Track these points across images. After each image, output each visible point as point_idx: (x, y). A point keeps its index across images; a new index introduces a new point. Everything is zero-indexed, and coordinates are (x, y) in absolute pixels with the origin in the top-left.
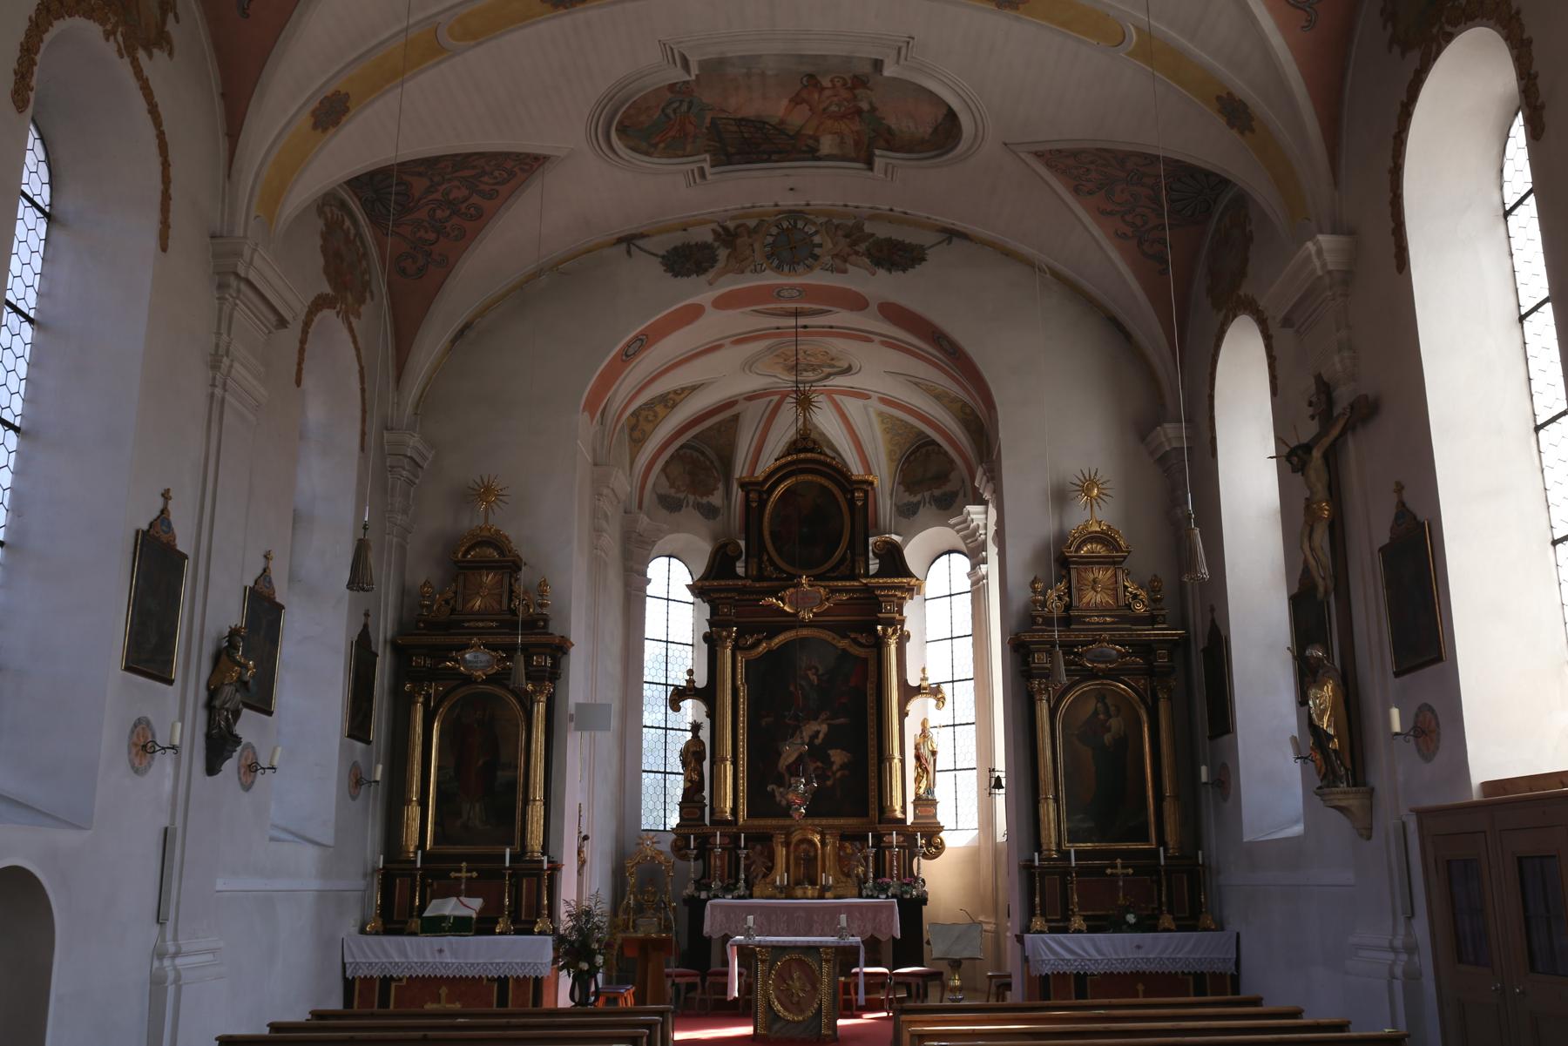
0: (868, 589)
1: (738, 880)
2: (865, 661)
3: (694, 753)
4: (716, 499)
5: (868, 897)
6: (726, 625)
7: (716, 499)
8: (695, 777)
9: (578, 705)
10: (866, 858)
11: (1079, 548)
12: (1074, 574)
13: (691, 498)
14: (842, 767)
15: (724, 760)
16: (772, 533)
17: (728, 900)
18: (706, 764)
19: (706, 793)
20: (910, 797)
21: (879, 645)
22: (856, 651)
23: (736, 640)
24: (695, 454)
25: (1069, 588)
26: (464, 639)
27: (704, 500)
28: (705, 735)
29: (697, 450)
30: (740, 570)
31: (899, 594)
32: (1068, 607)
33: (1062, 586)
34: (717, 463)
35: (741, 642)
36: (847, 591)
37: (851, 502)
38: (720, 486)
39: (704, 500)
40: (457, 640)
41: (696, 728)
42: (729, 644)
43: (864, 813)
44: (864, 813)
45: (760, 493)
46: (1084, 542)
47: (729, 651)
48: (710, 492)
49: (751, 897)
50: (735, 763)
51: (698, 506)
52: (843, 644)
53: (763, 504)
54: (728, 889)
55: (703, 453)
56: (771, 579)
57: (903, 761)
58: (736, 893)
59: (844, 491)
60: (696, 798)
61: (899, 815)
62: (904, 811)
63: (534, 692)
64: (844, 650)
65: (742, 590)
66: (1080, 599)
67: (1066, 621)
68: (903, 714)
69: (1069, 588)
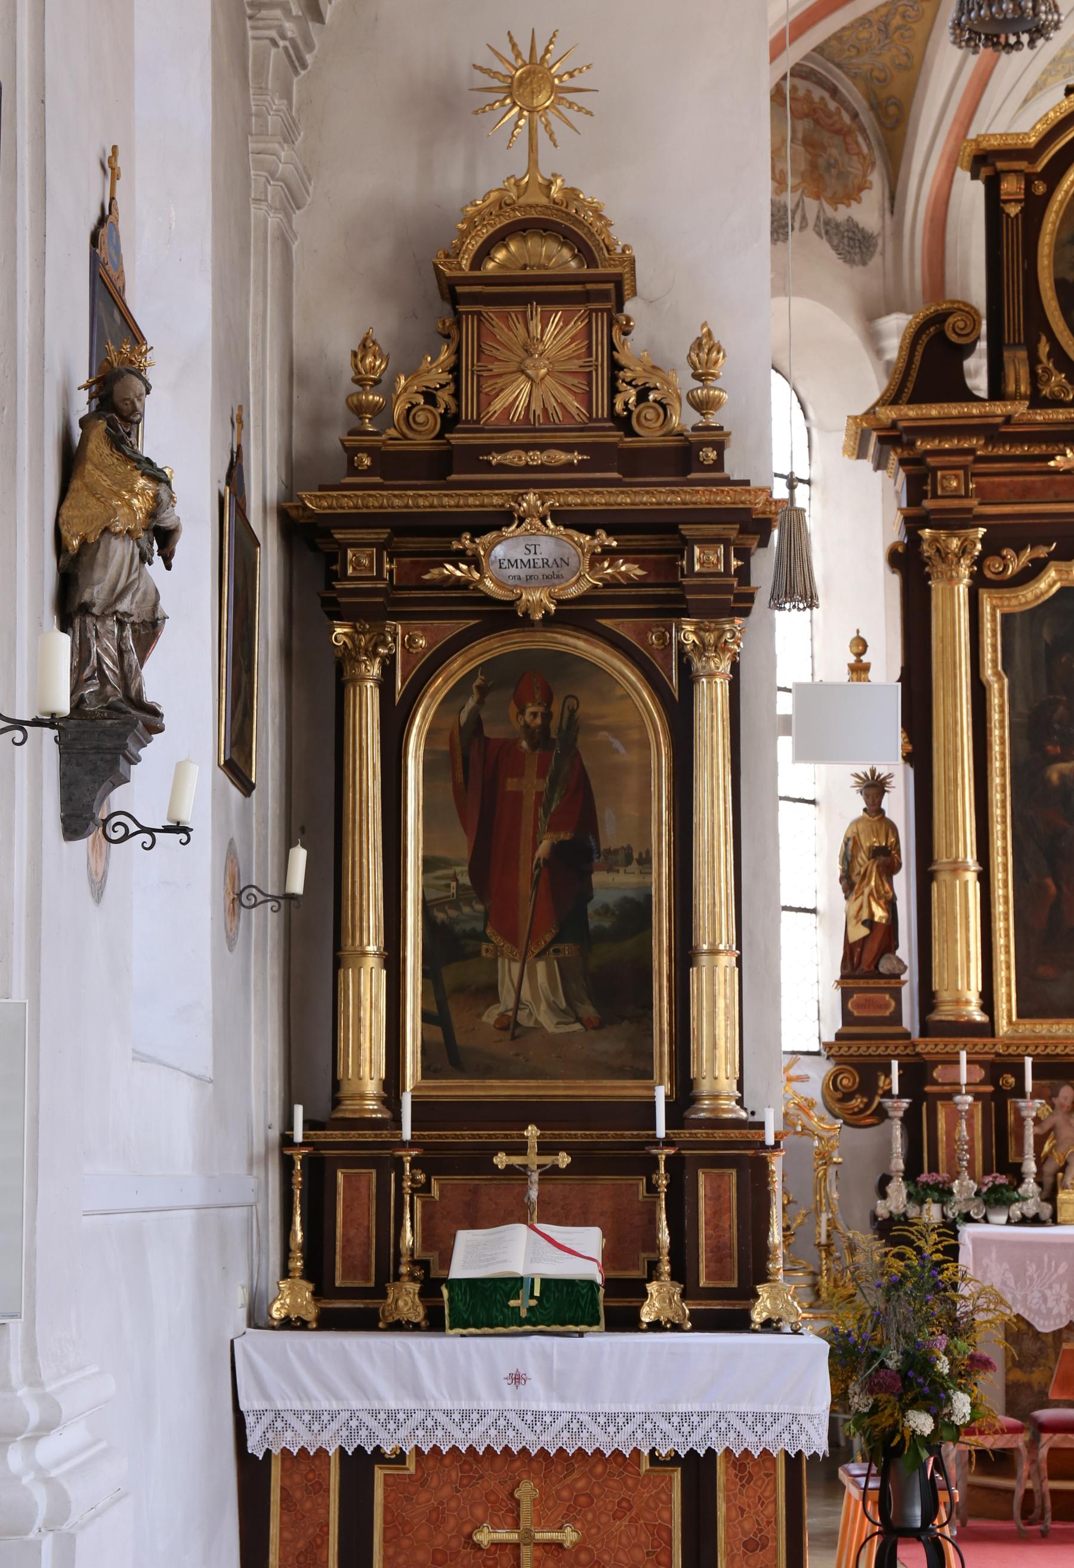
1: (1019, 1178)
3: (876, 853)
4: (867, 212)
6: (955, 521)
7: (867, 212)
8: (879, 914)
9: (800, 691)
13: (812, 206)
15: (957, 868)
16: (1060, 285)
17: (997, 1228)
18: (903, 884)
19: (906, 949)
23: (979, 562)
24: (818, 93)
26: (496, 500)
27: (841, 214)
28: (898, 806)
29: (821, 82)
30: (979, 382)
34: (866, 118)
35: (994, 566)
38: (876, 178)
39: (841, 214)
40: (473, 501)
41: (874, 788)
42: (964, 570)
45: (1029, 179)
47: (962, 590)
48: (851, 194)
49: (1054, 1220)
50: (985, 878)
51: (829, 230)
53: (1035, 208)
54: (996, 1198)
55: (834, 92)
56: (1056, 403)
58: (1016, 1210)
60: (885, 966)
63: (701, 649)
65: (991, 432)
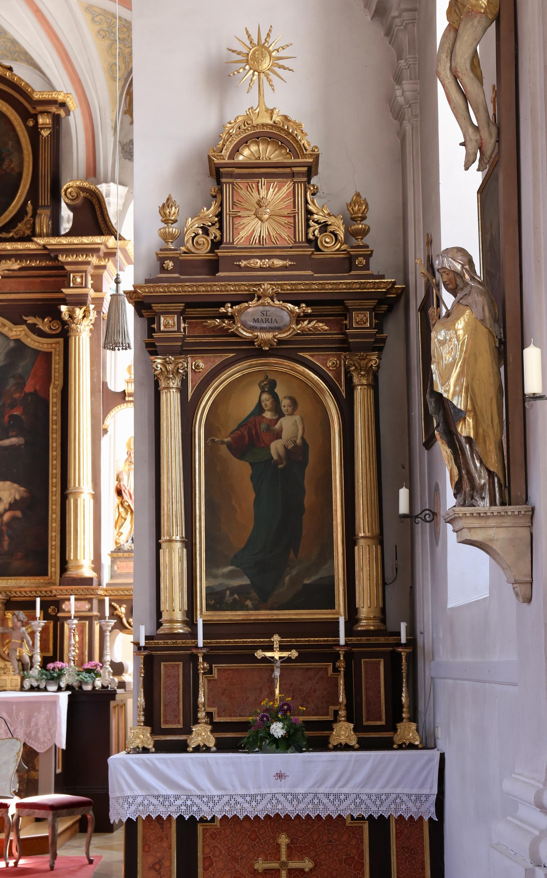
0: (49, 254)
2: (48, 356)
5: (32, 689)
10: (32, 634)
11: (236, 150)
12: (227, 189)
14: (13, 506)
20: (107, 547)
21: (65, 333)
22: (33, 342)
25: (220, 215)
31: (94, 260)
32: (216, 245)
33: (210, 212)
36: (18, 256)
37: (34, 132)
43: (43, 571)
44: (43, 571)
46: (245, 142)
52: (18, 332)
57: (97, 498)
59: (25, 115)
61: (87, 572)
62: (97, 565)
64: (18, 341)
66: (235, 230)
67: (213, 266)
68: (98, 431)
69: (220, 215)
